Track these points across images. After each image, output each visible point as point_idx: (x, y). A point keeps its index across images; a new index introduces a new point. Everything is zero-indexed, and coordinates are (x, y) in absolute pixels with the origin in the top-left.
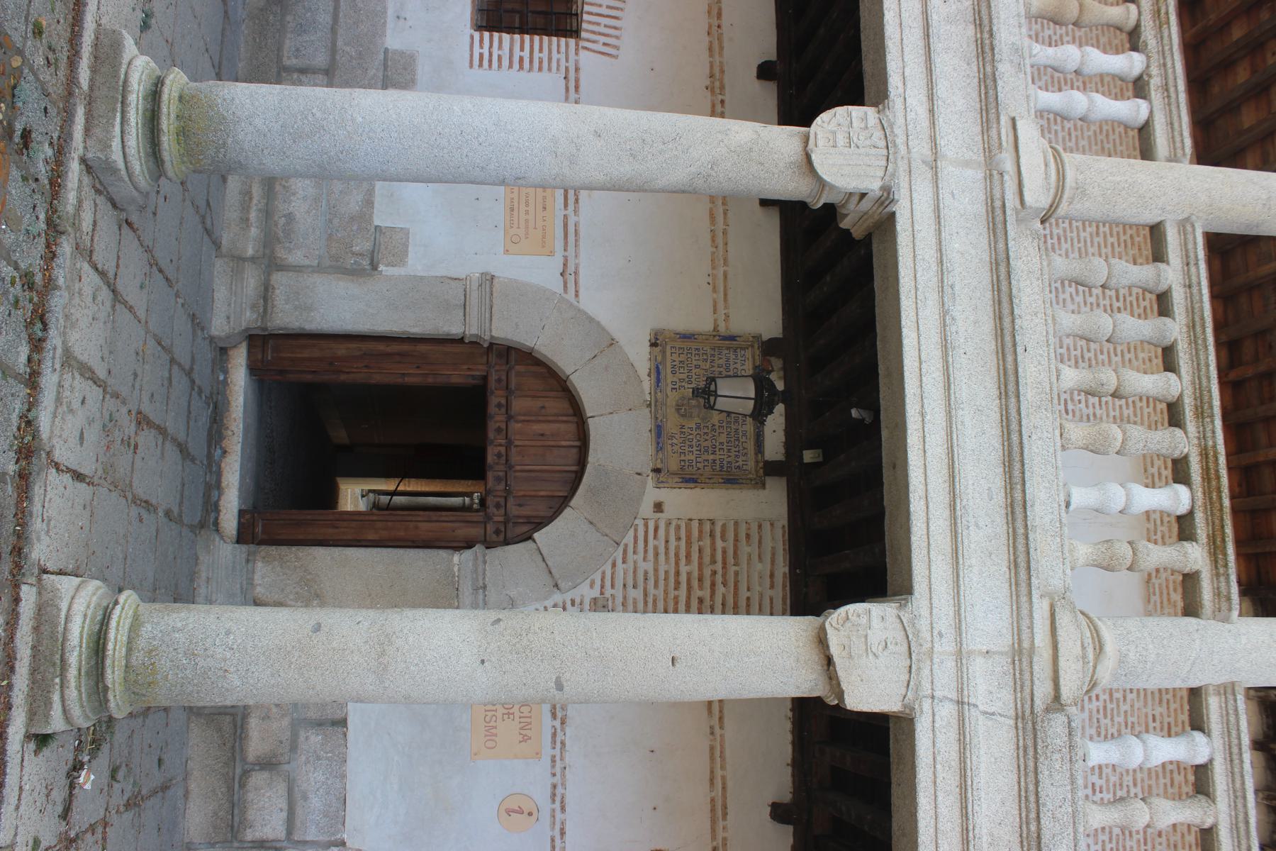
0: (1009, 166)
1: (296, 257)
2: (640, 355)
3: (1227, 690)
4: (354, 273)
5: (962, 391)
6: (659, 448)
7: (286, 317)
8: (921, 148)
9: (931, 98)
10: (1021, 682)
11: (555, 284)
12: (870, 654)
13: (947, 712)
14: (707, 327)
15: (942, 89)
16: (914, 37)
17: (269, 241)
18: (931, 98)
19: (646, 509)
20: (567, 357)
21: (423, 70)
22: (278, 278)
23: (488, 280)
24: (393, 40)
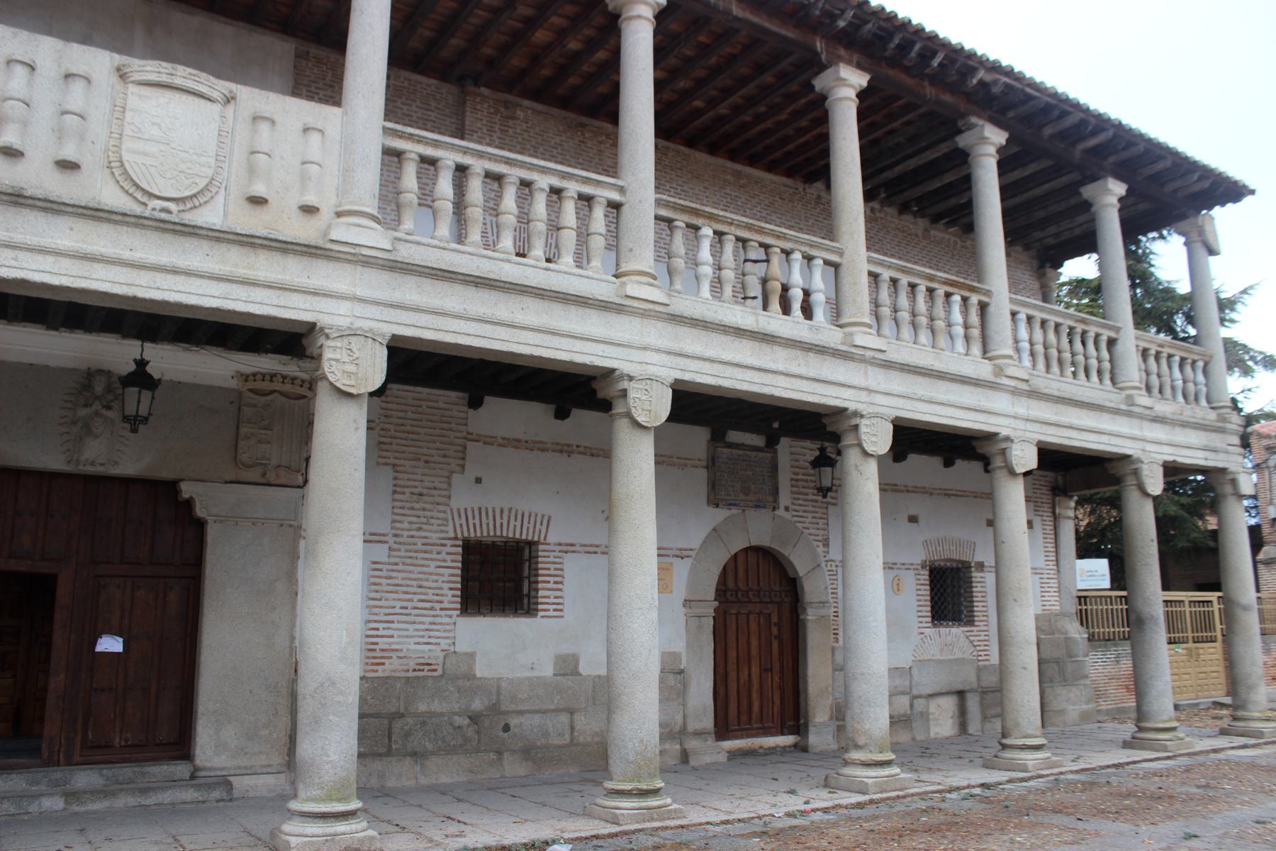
0: (870, 354)
1: (679, 719)
2: (721, 514)
4: (685, 685)
6: (765, 507)
7: (708, 722)
9: (843, 385)
11: (688, 561)
14: (702, 474)
15: (841, 379)
18: (843, 385)
19: (787, 515)
20: (724, 557)
21: (566, 649)
22: (693, 726)
23: (687, 603)
24: (547, 671)
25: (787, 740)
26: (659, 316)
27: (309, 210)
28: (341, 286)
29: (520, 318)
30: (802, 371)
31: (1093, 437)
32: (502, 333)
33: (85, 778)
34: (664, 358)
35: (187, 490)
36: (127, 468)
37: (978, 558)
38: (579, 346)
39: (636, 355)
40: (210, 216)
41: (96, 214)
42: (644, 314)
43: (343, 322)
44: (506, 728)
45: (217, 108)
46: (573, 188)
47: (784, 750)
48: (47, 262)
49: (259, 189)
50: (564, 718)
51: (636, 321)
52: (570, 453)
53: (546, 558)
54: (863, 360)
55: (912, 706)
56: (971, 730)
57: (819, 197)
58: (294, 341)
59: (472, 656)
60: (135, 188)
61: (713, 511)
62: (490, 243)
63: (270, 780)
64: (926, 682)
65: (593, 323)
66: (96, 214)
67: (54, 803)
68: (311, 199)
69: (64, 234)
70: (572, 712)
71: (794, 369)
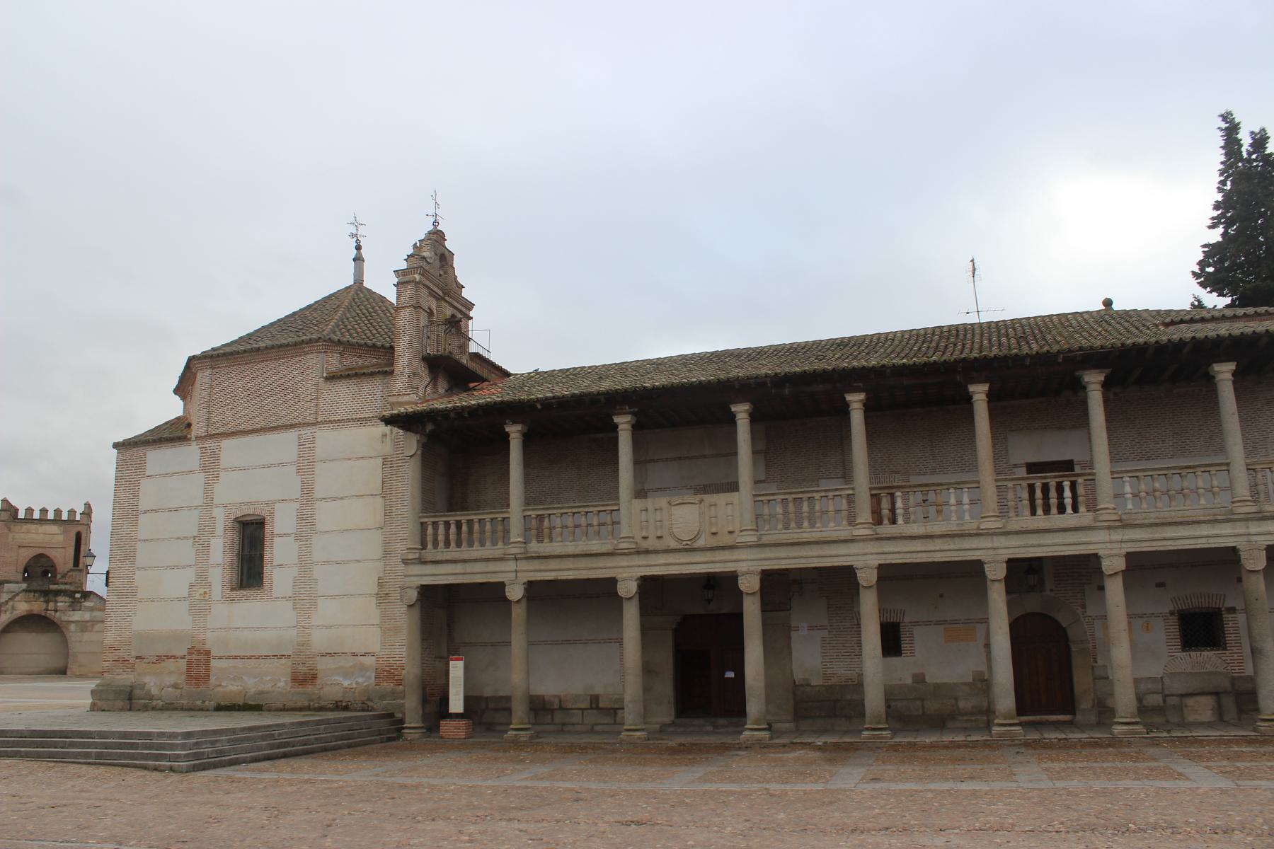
1: (985, 704)
5: (1049, 542)
8: (990, 552)
12: (1113, 563)
17: (981, 712)
24: (909, 681)
25: (1068, 717)
26: (871, 540)
27: (731, 532)
28: (743, 557)
29: (811, 554)
30: (952, 547)
31: (1191, 541)
32: (803, 561)
33: (721, 721)
36: (725, 611)
37: (1229, 604)
38: (836, 559)
39: (860, 558)
40: (701, 543)
41: (668, 551)
42: (863, 540)
43: (744, 569)
47: (1064, 723)
49: (714, 530)
50: (919, 703)
53: (904, 630)
54: (988, 534)
55: (1164, 701)
56: (1226, 718)
58: (732, 578)
60: (678, 540)
62: (799, 526)
63: (787, 725)
64: (1178, 686)
66: (668, 551)
67: (710, 728)
68: (731, 529)
69: (661, 559)
70: (922, 700)
71: (946, 547)
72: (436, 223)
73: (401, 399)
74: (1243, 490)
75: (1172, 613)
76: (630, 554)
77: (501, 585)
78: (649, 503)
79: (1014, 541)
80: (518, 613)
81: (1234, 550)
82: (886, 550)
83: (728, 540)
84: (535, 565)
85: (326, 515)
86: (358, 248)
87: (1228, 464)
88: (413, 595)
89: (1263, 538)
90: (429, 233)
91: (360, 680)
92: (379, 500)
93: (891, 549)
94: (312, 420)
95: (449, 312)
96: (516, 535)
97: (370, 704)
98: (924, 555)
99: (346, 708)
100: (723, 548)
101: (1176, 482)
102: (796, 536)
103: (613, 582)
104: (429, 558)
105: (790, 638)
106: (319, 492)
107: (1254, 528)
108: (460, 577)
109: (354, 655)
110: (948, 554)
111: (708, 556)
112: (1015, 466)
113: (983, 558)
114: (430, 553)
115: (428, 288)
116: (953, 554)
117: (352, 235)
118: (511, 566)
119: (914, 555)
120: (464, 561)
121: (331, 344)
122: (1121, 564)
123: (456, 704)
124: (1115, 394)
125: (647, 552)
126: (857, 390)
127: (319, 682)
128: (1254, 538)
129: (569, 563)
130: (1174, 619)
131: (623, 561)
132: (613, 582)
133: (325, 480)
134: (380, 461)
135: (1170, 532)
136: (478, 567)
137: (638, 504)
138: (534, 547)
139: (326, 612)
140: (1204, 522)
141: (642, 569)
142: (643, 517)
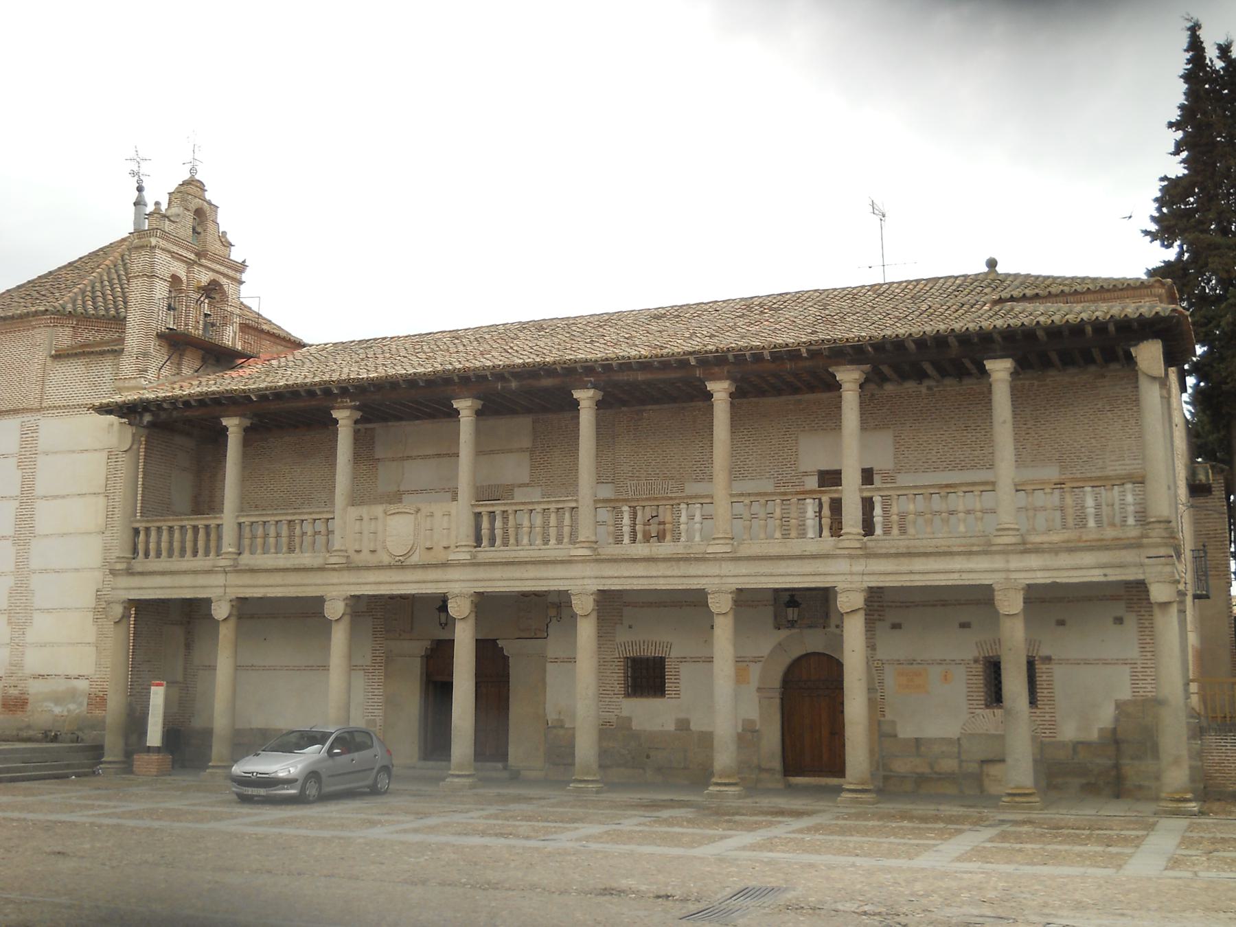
2: (784, 633)
3: (861, 490)
7: (777, 764)
8: (717, 580)
10: (858, 557)
13: (865, 578)
14: (771, 608)
15: (700, 573)
16: (685, 581)
21: (682, 716)
23: (759, 690)
24: (671, 727)
26: (588, 561)
29: (526, 575)
31: (942, 576)
34: (594, 581)
35: (500, 643)
38: (552, 582)
39: (580, 582)
40: (415, 559)
42: (583, 562)
43: (457, 591)
44: (648, 757)
45: (412, 517)
46: (553, 506)
48: (368, 587)
51: (580, 565)
52: (681, 607)
53: (669, 666)
54: (715, 559)
57: (873, 395)
58: (442, 603)
59: (629, 719)
60: (391, 554)
61: (777, 631)
65: (559, 571)
69: (372, 577)
71: (669, 573)
72: (193, 170)
73: (127, 384)
74: (1006, 517)
75: (976, 661)
76: (340, 570)
77: (207, 602)
78: (364, 511)
79: (744, 568)
80: (226, 633)
81: (989, 589)
82: (606, 574)
83: (441, 556)
84: (246, 579)
85: (47, 517)
86: (140, 189)
87: (993, 483)
88: (118, 610)
89: (1023, 575)
90: (184, 184)
91: (72, 707)
92: (102, 501)
93: (610, 573)
94: (37, 405)
95: (204, 278)
96: (228, 547)
97: (80, 734)
98: (645, 581)
99: (55, 739)
100: (436, 566)
101: (937, 503)
102: (513, 554)
103: (320, 601)
104: (140, 570)
105: (545, 671)
106: (40, 490)
107: (1016, 562)
108: (168, 591)
109: (68, 677)
110: (671, 580)
111: (419, 575)
112: (806, 474)
113: (709, 589)
114: (138, 565)
115: (169, 252)
116: (676, 581)
117: (133, 173)
118: (219, 580)
119: (635, 581)
120: (172, 573)
121: (61, 316)
122: (858, 600)
123: (154, 736)
124: (929, 388)
125: (358, 568)
126: (584, 387)
127: (29, 707)
128: (1014, 576)
129: (277, 579)
130: (979, 668)
131: (334, 578)
132: (320, 601)
133: (48, 475)
134: (105, 454)
135: (919, 565)
136: (187, 580)
137: (353, 512)
138: (246, 559)
139: (42, 627)
140: (959, 553)
141: (352, 587)
142: (357, 527)
